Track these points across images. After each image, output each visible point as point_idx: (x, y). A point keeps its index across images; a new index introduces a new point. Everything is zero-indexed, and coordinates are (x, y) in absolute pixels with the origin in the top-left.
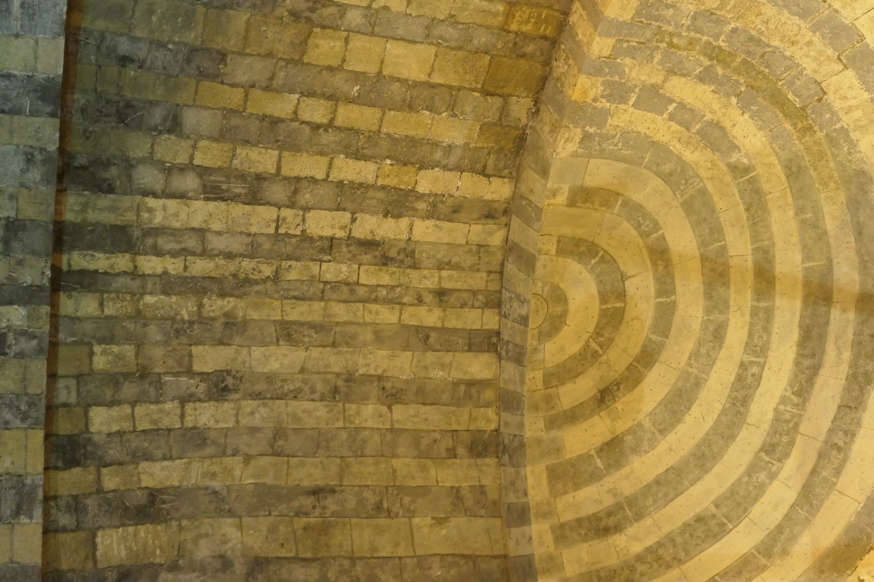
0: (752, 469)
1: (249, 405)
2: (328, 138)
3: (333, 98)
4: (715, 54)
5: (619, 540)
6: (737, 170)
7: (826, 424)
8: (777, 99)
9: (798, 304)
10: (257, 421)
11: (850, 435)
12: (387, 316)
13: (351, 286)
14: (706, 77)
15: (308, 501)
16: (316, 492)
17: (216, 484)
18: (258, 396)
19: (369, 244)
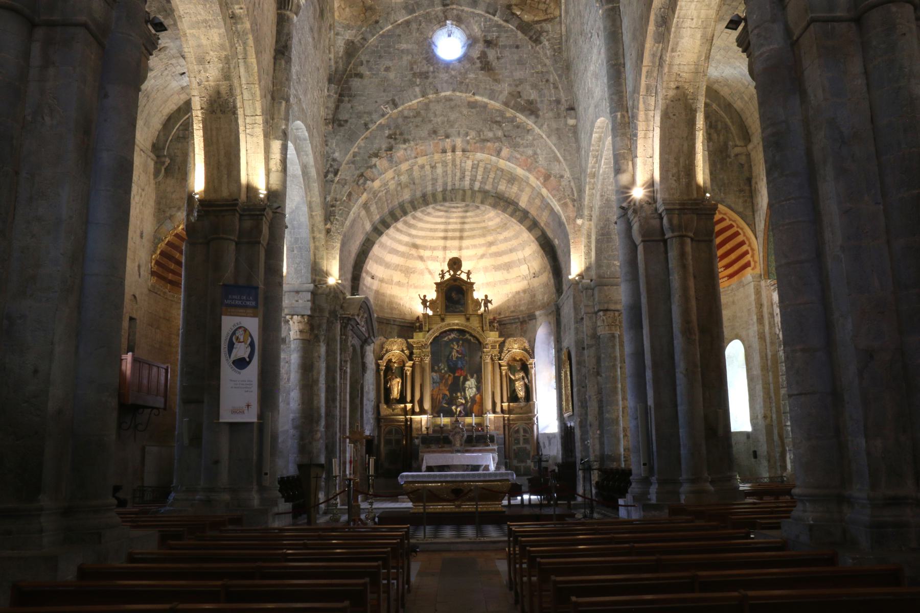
0: (427, 229)
1: (430, 171)
2: (486, 177)
3: (494, 179)
4: (506, 224)
5: (412, 220)
6: (484, 221)
7: (437, 235)
8: (498, 228)
9: (459, 228)
10: (427, 173)
11: (436, 239)
12: (450, 180)
13: (456, 176)
14: (502, 222)
15: (412, 183)
16: (414, 183)
17: (414, 173)
18: (432, 171)
19: (464, 177)
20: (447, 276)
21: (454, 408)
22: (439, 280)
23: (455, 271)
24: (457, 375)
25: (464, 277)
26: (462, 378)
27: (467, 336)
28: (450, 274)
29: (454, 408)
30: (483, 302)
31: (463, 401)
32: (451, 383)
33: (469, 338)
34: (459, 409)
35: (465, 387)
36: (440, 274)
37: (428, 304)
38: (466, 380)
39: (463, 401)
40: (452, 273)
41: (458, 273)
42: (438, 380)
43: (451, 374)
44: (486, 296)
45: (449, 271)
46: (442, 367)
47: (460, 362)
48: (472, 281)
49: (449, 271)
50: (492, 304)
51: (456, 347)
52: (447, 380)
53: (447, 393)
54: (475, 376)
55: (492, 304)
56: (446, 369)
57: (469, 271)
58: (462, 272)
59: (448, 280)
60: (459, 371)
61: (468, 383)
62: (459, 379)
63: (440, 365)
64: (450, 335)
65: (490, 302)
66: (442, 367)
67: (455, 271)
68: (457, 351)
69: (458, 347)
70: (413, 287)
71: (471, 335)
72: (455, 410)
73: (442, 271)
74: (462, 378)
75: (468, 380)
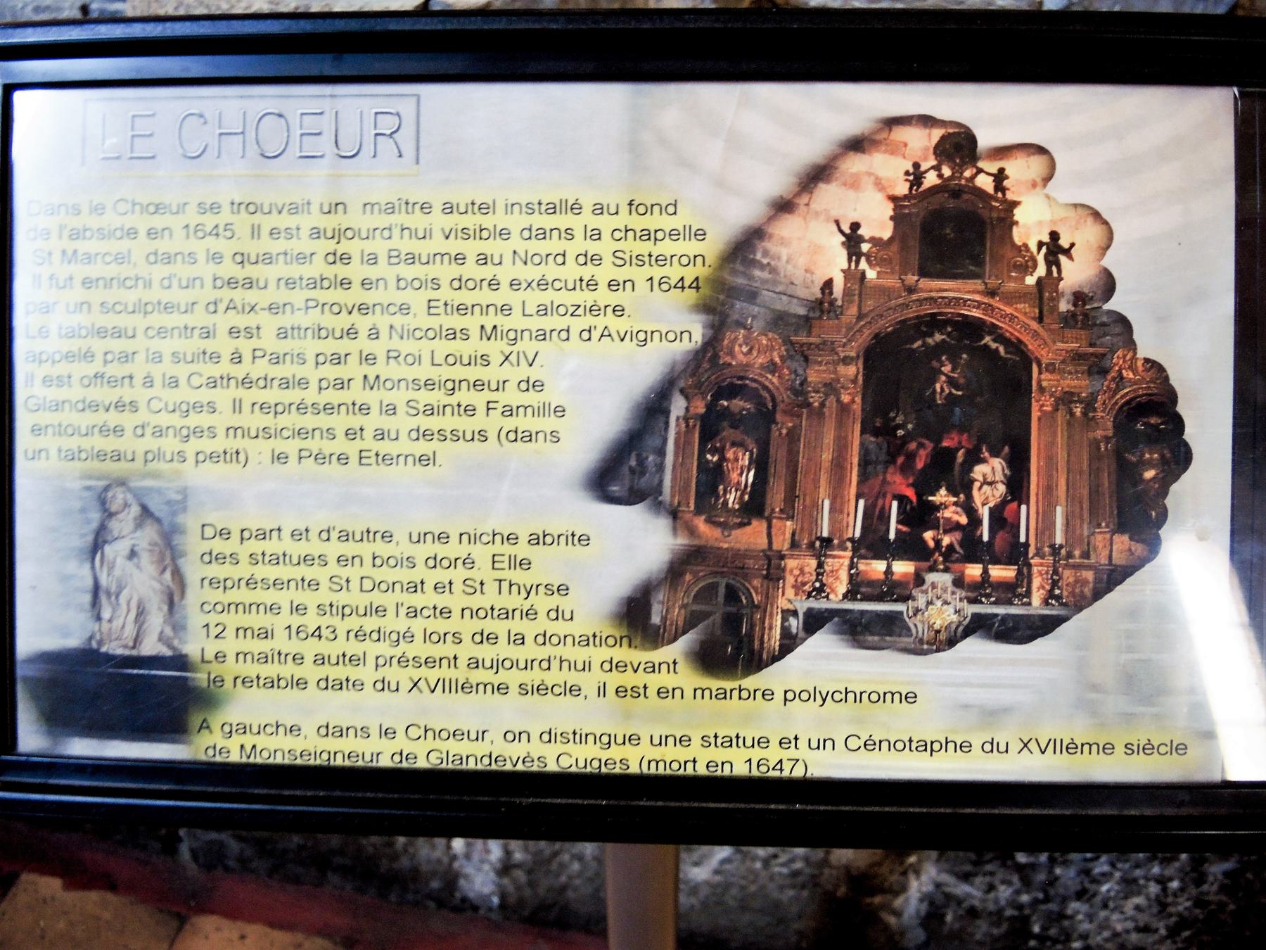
20: (931, 179)
21: (928, 535)
22: (902, 189)
23: (958, 170)
24: (945, 444)
25: (985, 183)
26: (961, 453)
27: (987, 339)
28: (940, 176)
29: (928, 535)
30: (1044, 250)
31: (964, 520)
32: (924, 469)
33: (994, 346)
34: (946, 540)
35: (972, 481)
36: (907, 173)
37: (865, 247)
38: (974, 458)
39: (964, 520)
40: (947, 172)
41: (967, 174)
42: (883, 457)
43: (926, 442)
44: (1054, 236)
45: (937, 168)
46: (899, 420)
47: (957, 410)
48: (1010, 196)
49: (937, 168)
50: (1071, 258)
51: (947, 369)
52: (911, 457)
53: (910, 493)
54: (1007, 449)
55: (1071, 258)
56: (910, 426)
57: (1002, 170)
58: (980, 171)
59: (934, 190)
60: (954, 435)
61: (979, 471)
62: (955, 458)
63: (892, 414)
64: (931, 335)
65: (1067, 252)
66: (899, 420)
67: (958, 170)
68: (951, 382)
69: (953, 370)
70: (823, 217)
71: (1000, 338)
72: (931, 544)
73: (916, 166)
74: (961, 453)
75: (984, 461)
